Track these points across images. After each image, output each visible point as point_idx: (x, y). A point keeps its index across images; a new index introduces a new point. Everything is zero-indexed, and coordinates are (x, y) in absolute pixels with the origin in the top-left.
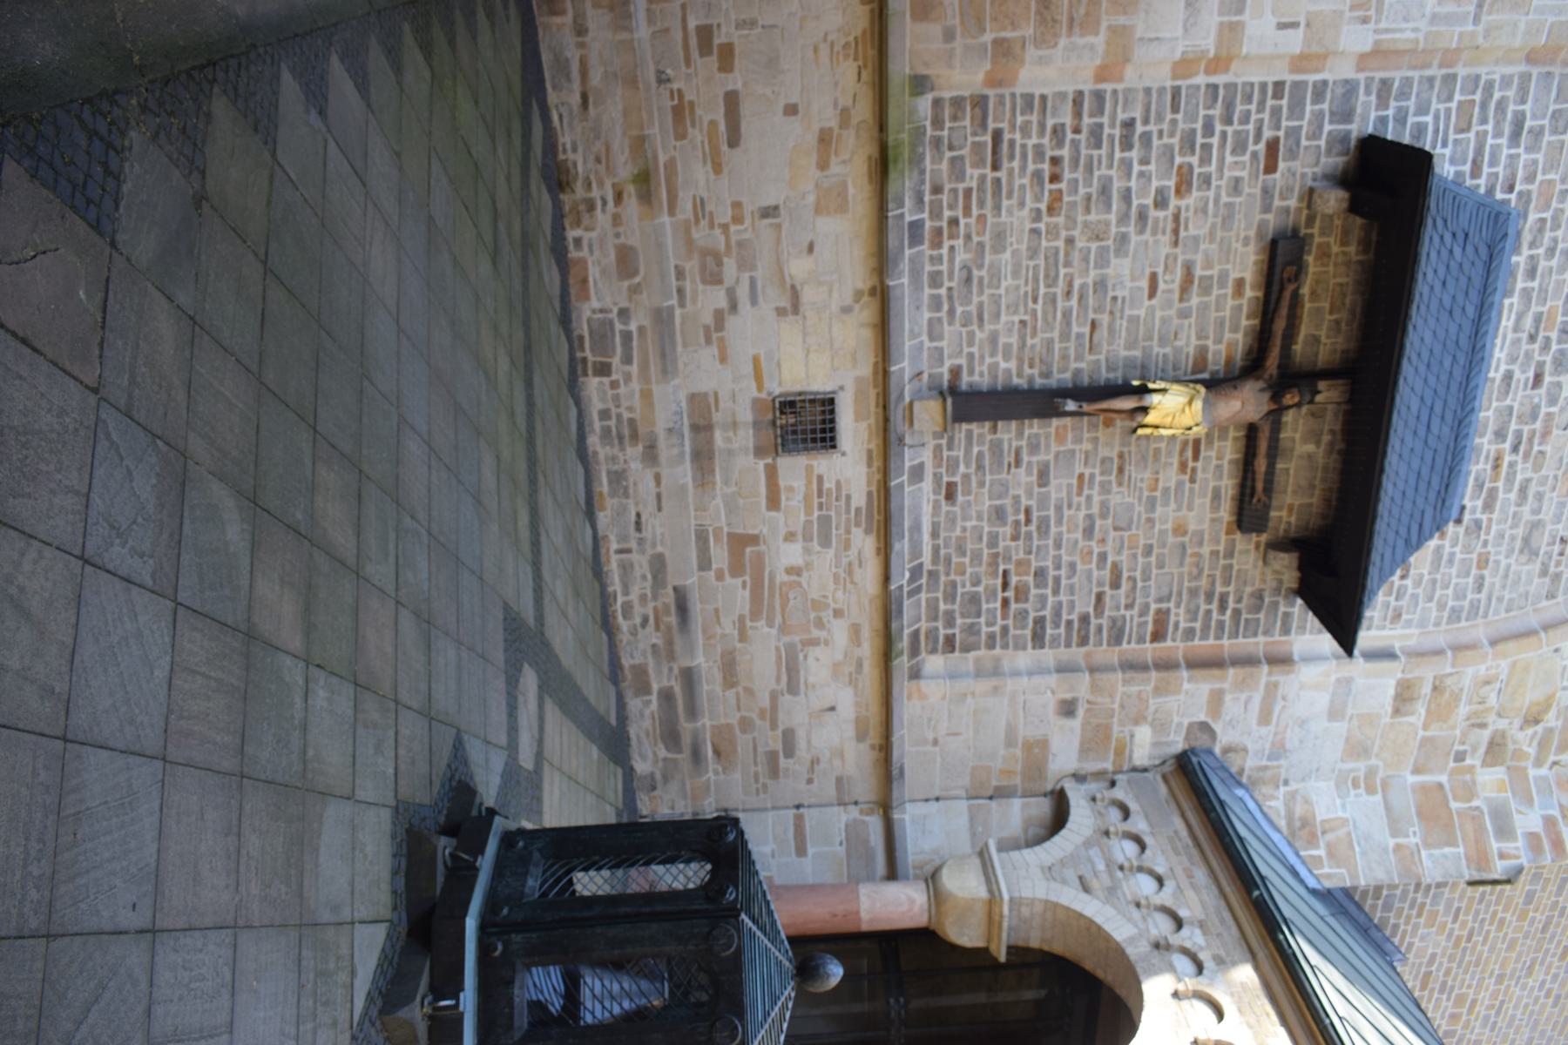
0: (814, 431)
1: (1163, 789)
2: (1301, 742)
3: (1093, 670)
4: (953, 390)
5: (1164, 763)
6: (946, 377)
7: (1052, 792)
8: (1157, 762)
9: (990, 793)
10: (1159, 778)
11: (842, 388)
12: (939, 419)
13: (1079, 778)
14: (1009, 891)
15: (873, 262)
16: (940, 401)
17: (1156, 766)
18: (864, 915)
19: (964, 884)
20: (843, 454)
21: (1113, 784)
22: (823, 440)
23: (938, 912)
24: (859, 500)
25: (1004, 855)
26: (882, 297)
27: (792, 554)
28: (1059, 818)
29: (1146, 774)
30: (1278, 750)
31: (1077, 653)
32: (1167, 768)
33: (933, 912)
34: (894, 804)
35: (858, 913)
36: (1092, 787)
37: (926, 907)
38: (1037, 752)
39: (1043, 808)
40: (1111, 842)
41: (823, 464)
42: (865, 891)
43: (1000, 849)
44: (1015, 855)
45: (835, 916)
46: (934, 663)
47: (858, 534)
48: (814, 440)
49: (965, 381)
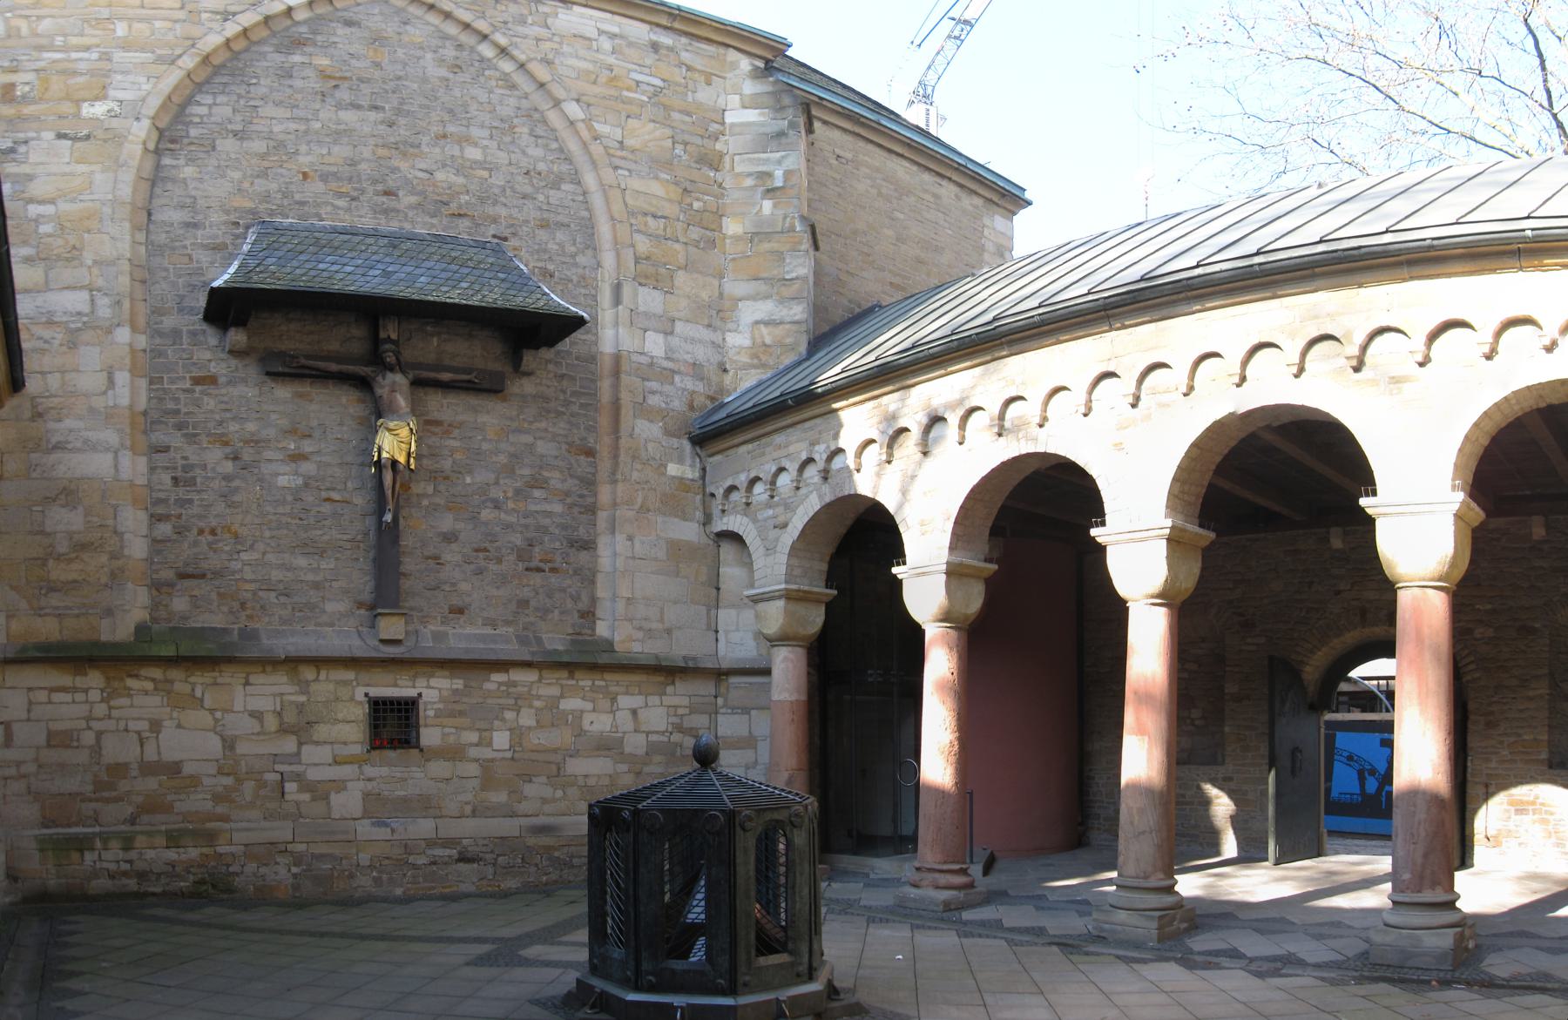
0: (400, 718)
1: (718, 458)
2: (688, 353)
3: (615, 504)
4: (372, 607)
5: (697, 454)
6: (362, 612)
7: (716, 542)
8: (698, 460)
9: (715, 591)
10: (711, 460)
11: (366, 695)
12: (394, 619)
13: (707, 520)
14: (781, 583)
15: (269, 669)
16: (379, 617)
17: (701, 460)
18: (793, 698)
19: (775, 616)
20: (420, 695)
21: (713, 495)
22: (407, 711)
23: (794, 639)
24: (458, 684)
25: (756, 584)
26: (293, 663)
27: (501, 739)
28: (735, 538)
29: (708, 469)
30: (696, 369)
31: (602, 516)
32: (703, 454)
33: (795, 643)
34: (718, 666)
35: (791, 702)
36: (716, 512)
37: (790, 648)
38: (678, 551)
39: (728, 551)
40: (754, 502)
41: (427, 712)
42: (776, 695)
43: (752, 586)
44: (757, 575)
45: (793, 720)
46: (602, 629)
47: (489, 686)
48: (407, 718)
49: (367, 596)
